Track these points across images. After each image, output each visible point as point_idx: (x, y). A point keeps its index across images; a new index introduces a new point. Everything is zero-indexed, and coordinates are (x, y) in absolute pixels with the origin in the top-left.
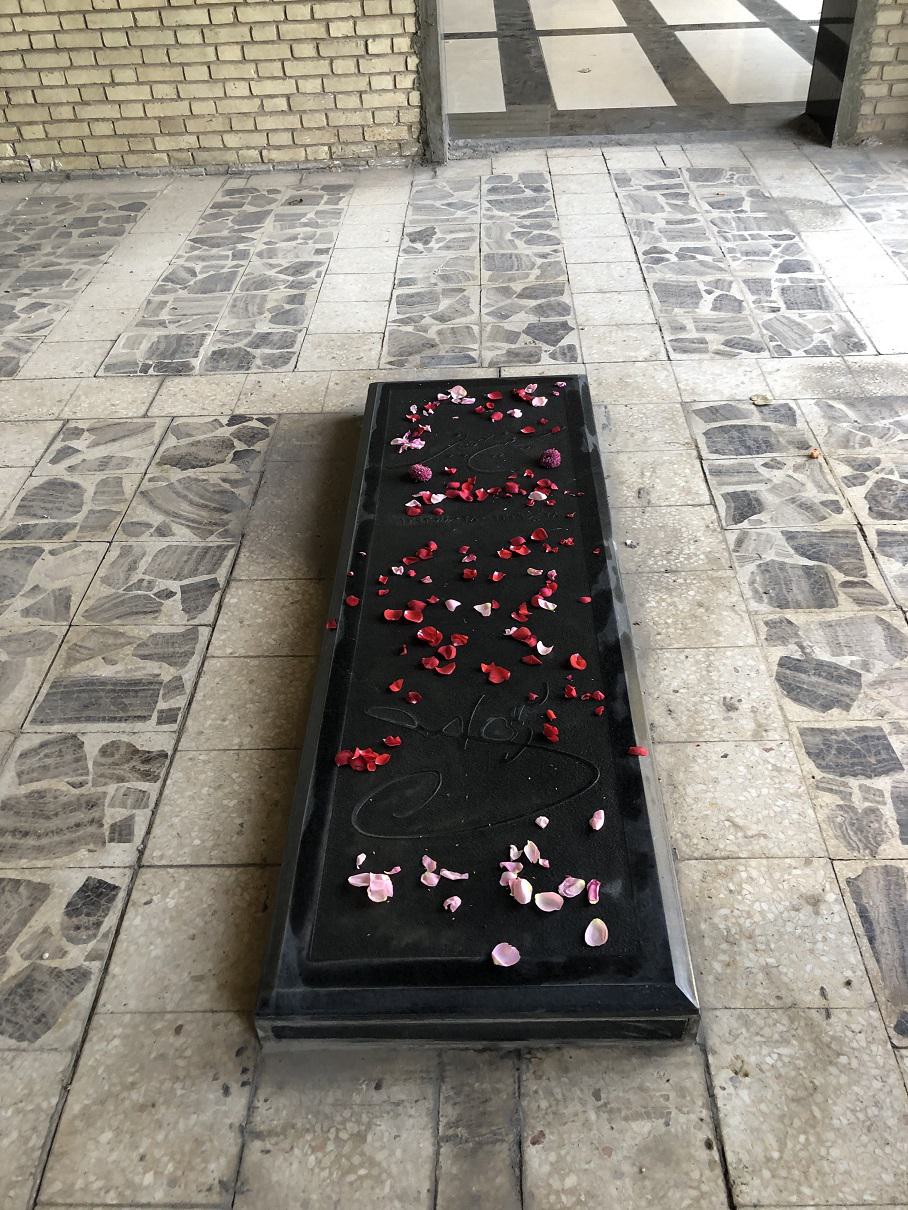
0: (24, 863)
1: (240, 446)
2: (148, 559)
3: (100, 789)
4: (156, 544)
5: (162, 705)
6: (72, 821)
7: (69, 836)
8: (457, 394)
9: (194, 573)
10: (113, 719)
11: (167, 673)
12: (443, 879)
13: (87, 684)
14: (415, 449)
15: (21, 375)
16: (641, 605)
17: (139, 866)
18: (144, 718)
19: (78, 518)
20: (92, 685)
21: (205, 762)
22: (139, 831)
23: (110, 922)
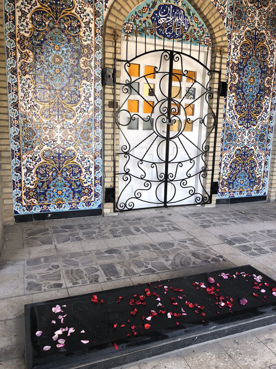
0: (65, 276)
1: (210, 260)
2: (157, 261)
3: (86, 278)
4: (162, 260)
5: (112, 277)
6: (76, 277)
7: (73, 278)
8: (258, 278)
9: (155, 268)
10: (105, 273)
11: (122, 274)
12: (61, 319)
13: (114, 267)
14: (223, 278)
15: (206, 229)
16: (205, 351)
17: (67, 288)
18: (107, 276)
19: (162, 249)
20: (114, 267)
21: (98, 288)
22: (76, 285)
23: (53, 289)
